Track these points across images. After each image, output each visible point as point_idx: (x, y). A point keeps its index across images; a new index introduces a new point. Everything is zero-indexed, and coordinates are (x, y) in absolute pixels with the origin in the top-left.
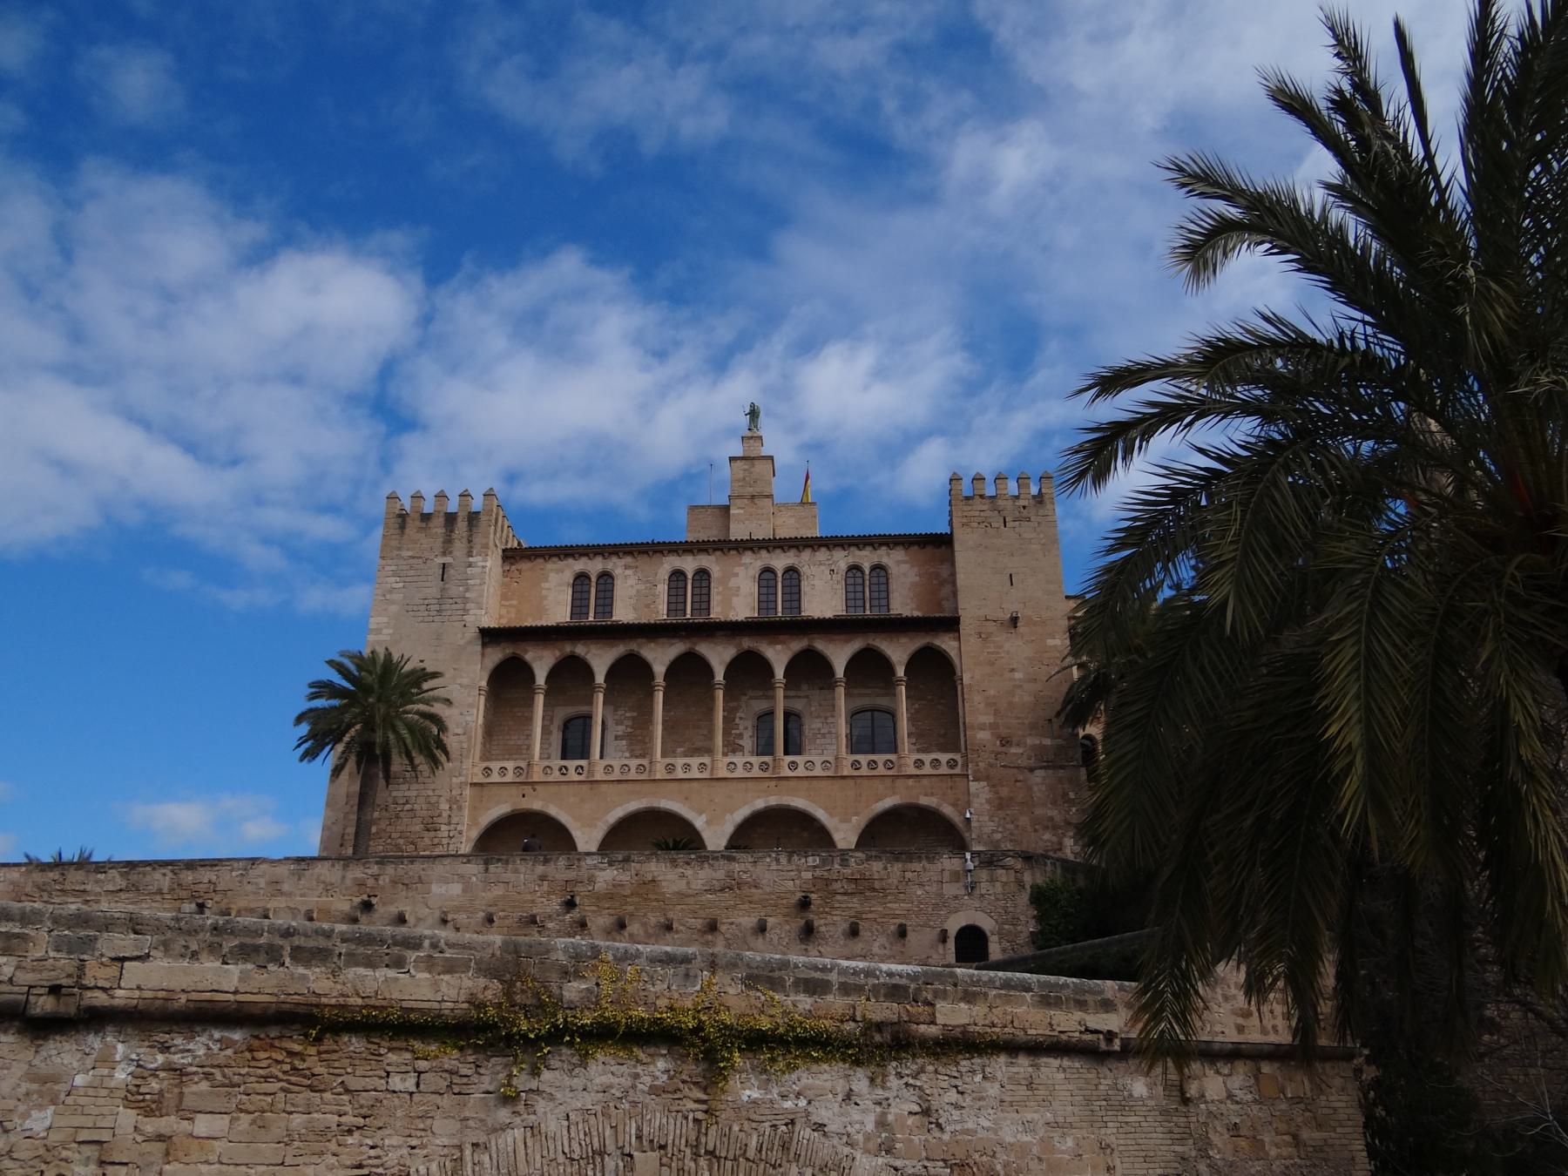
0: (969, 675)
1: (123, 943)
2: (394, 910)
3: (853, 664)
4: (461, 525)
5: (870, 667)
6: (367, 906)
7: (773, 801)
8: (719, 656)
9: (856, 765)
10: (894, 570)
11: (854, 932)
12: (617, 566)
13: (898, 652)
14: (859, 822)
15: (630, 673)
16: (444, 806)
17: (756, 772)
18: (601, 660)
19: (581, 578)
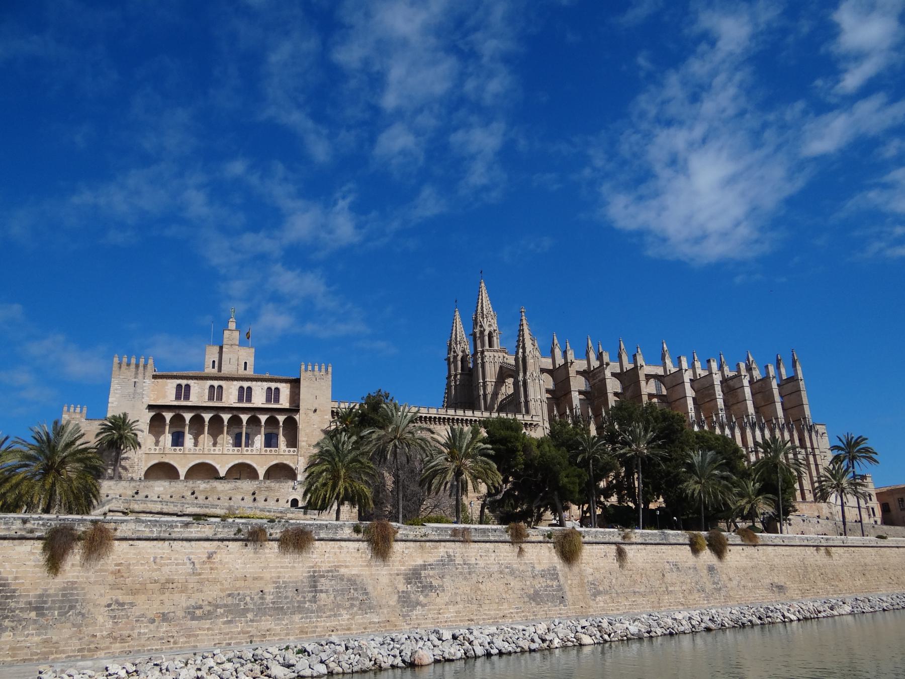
0: (301, 426)
1: (186, 506)
2: (145, 494)
3: (267, 421)
4: (141, 368)
5: (272, 421)
6: (137, 493)
7: (240, 461)
8: (226, 417)
9: (266, 451)
10: (281, 390)
11: (266, 500)
12: (191, 382)
13: (281, 418)
14: (266, 468)
15: (197, 421)
16: (136, 460)
17: (236, 452)
18: (188, 416)
19: (179, 386)
